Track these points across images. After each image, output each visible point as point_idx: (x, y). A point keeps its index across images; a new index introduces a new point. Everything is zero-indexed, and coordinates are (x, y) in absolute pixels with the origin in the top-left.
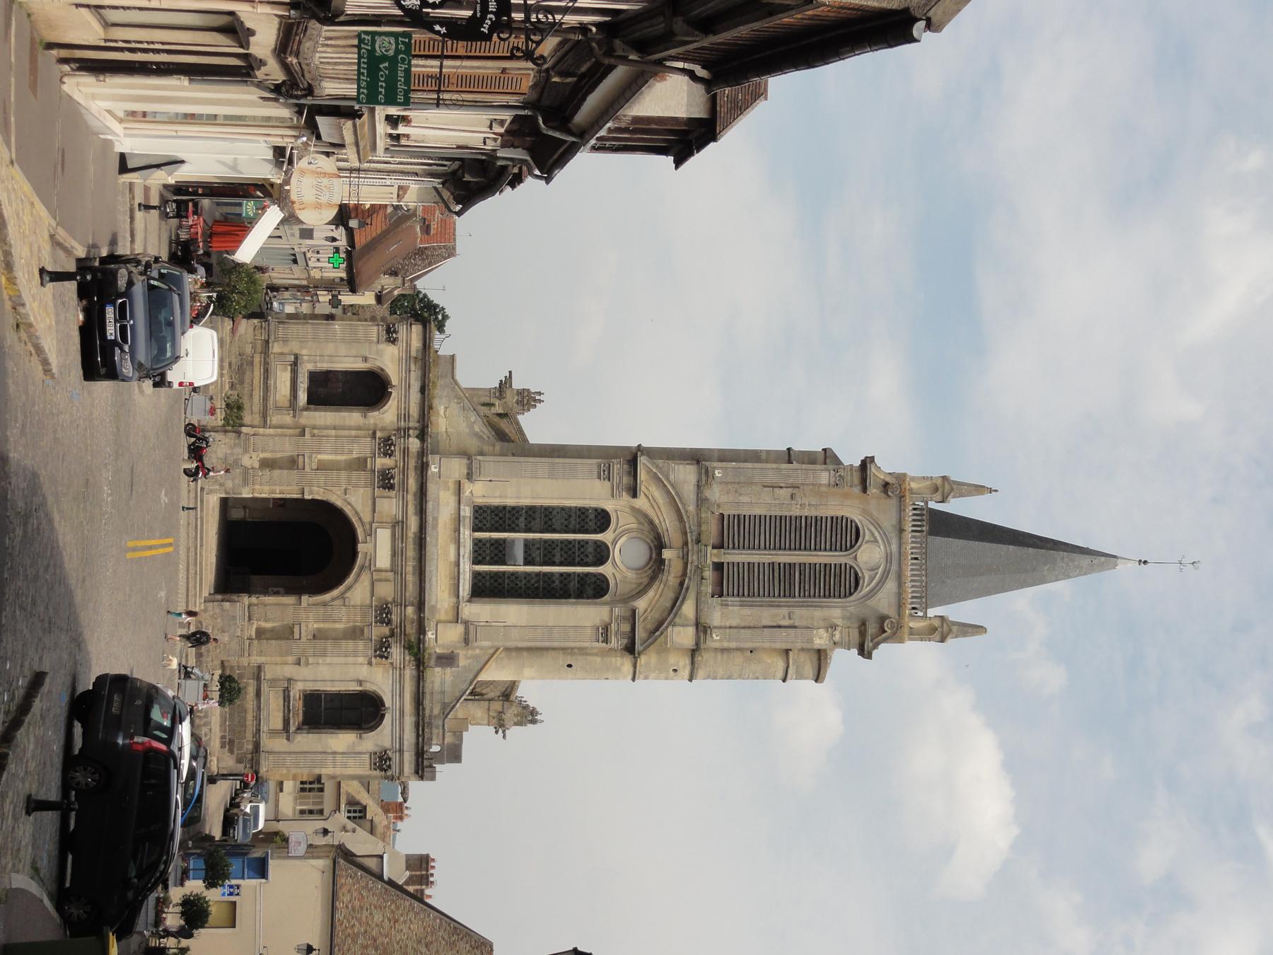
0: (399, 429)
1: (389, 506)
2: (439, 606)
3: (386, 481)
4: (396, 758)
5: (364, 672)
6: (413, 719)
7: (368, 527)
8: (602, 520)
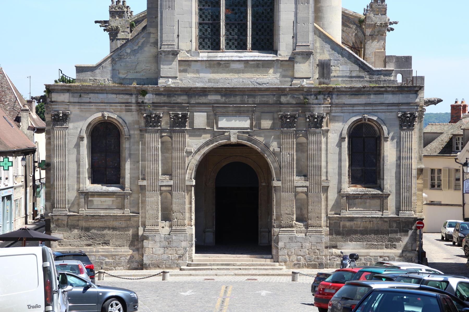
6: (372, 96)
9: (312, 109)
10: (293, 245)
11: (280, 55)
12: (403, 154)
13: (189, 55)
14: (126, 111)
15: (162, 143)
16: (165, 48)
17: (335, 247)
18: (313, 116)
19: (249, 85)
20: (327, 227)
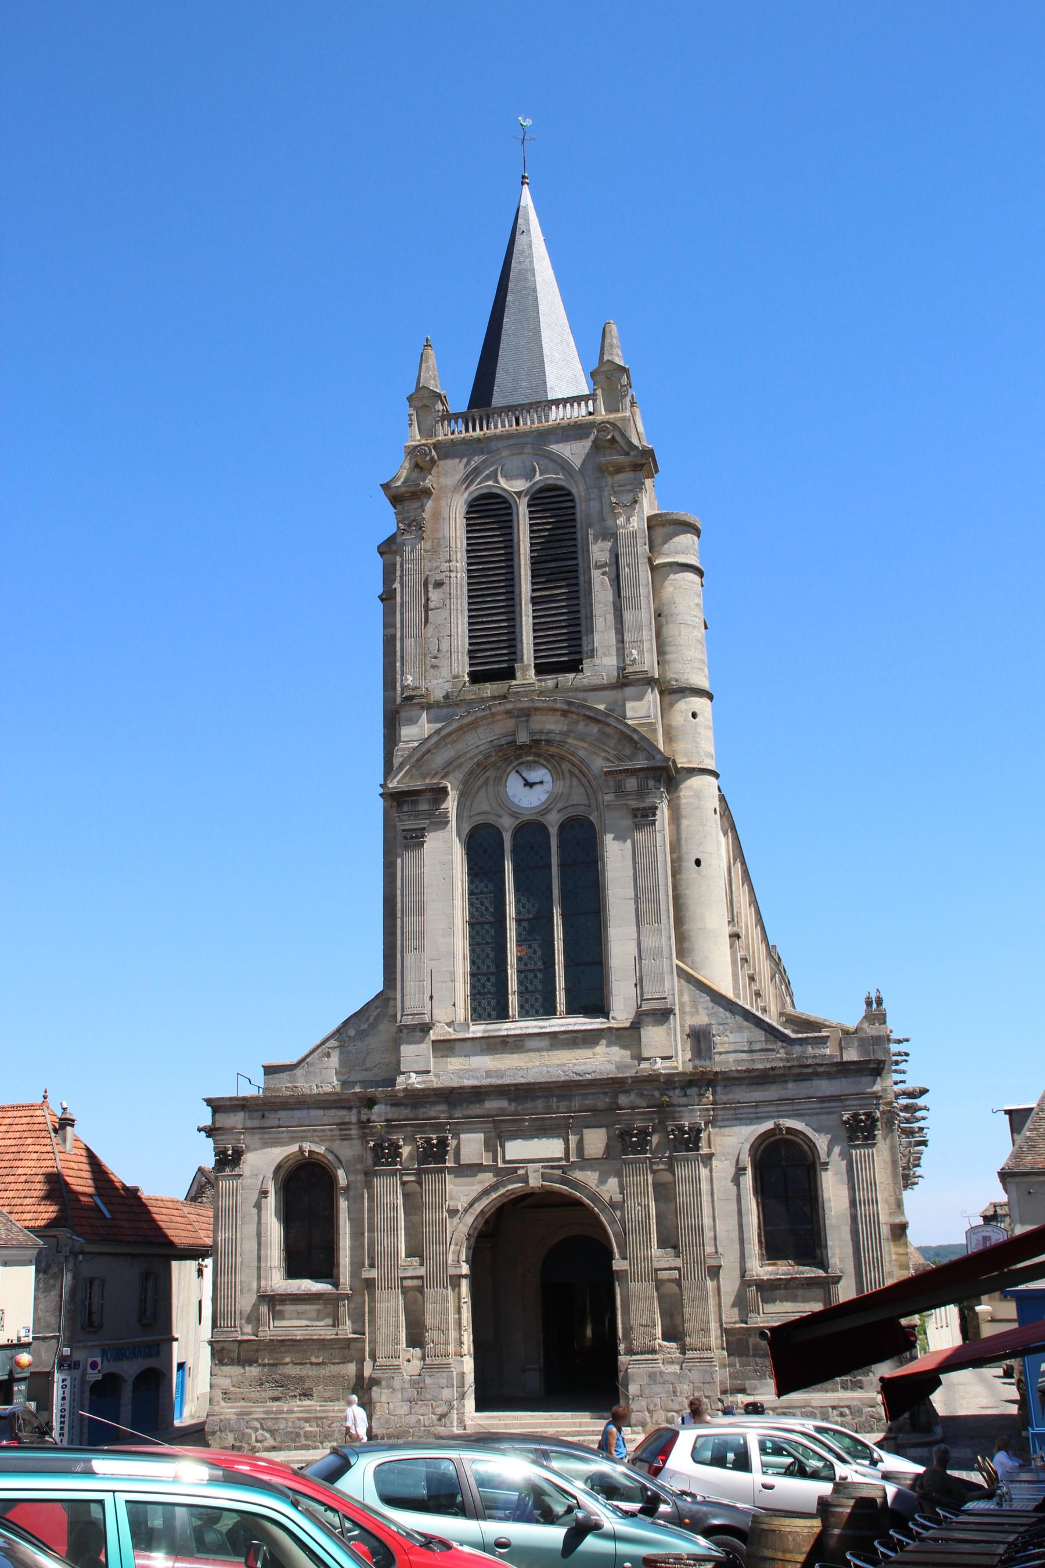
0: (364, 1138)
2: (618, 1059)
6: (790, 1085)
9: (677, 1115)
10: (657, 1388)
11: (614, 1018)
12: (860, 1195)
13: (451, 1030)
14: (342, 1139)
15: (406, 1195)
16: (408, 1021)
17: (742, 1391)
18: (680, 1128)
19: (559, 1076)
20: (723, 1349)
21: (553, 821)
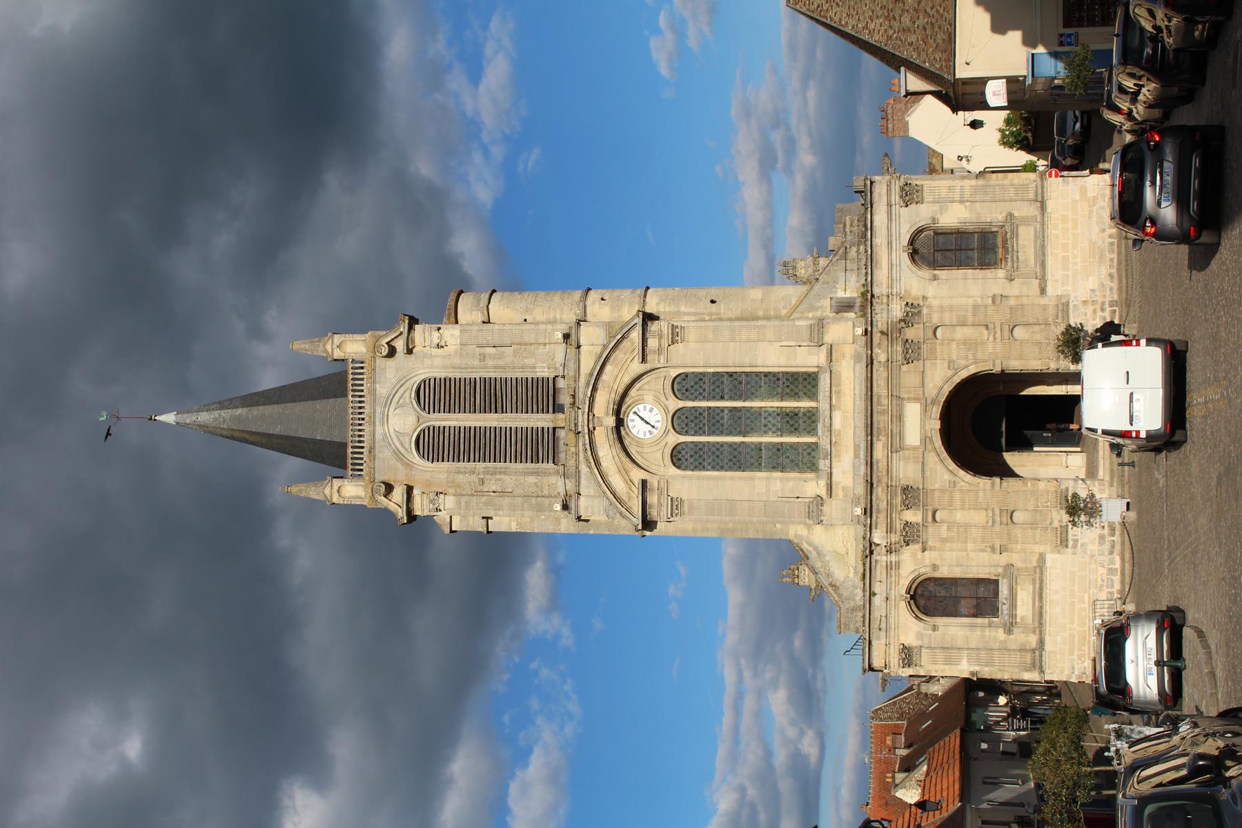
1: (906, 472)
3: (910, 496)
4: (895, 198)
5: (932, 290)
6: (877, 241)
7: (929, 447)
8: (678, 457)
21: (674, 404)
